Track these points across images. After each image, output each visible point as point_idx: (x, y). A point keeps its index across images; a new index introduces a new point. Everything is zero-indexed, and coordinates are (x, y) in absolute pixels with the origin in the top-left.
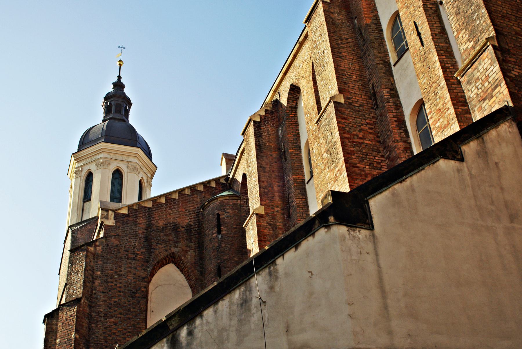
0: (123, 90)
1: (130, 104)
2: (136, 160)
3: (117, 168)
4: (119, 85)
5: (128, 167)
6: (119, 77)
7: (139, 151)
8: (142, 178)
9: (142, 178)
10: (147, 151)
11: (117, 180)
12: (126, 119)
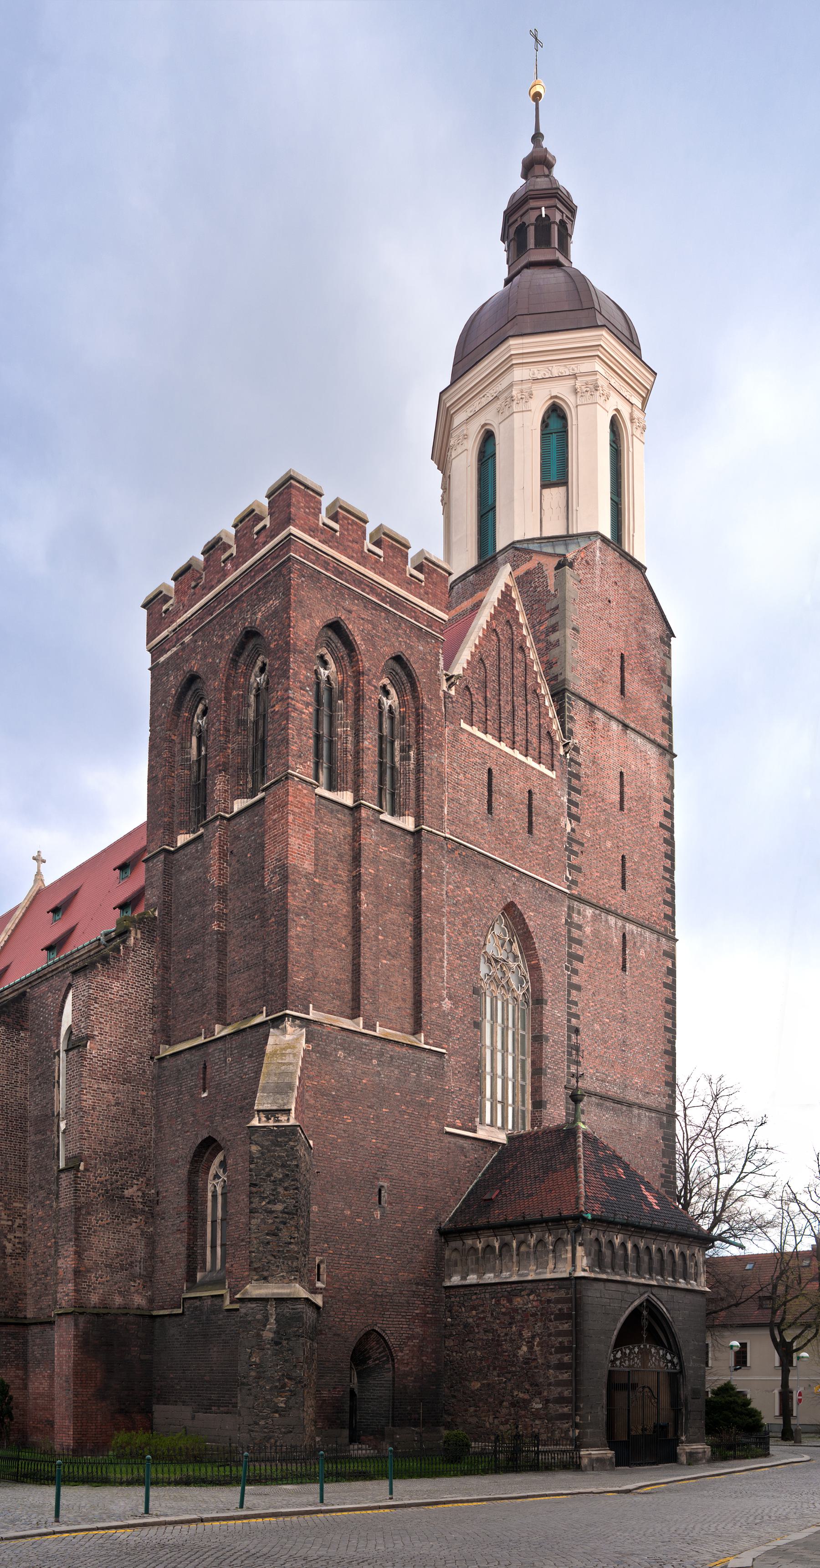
2: (598, 366)
7: (605, 338)
8: (617, 410)
10: (627, 334)
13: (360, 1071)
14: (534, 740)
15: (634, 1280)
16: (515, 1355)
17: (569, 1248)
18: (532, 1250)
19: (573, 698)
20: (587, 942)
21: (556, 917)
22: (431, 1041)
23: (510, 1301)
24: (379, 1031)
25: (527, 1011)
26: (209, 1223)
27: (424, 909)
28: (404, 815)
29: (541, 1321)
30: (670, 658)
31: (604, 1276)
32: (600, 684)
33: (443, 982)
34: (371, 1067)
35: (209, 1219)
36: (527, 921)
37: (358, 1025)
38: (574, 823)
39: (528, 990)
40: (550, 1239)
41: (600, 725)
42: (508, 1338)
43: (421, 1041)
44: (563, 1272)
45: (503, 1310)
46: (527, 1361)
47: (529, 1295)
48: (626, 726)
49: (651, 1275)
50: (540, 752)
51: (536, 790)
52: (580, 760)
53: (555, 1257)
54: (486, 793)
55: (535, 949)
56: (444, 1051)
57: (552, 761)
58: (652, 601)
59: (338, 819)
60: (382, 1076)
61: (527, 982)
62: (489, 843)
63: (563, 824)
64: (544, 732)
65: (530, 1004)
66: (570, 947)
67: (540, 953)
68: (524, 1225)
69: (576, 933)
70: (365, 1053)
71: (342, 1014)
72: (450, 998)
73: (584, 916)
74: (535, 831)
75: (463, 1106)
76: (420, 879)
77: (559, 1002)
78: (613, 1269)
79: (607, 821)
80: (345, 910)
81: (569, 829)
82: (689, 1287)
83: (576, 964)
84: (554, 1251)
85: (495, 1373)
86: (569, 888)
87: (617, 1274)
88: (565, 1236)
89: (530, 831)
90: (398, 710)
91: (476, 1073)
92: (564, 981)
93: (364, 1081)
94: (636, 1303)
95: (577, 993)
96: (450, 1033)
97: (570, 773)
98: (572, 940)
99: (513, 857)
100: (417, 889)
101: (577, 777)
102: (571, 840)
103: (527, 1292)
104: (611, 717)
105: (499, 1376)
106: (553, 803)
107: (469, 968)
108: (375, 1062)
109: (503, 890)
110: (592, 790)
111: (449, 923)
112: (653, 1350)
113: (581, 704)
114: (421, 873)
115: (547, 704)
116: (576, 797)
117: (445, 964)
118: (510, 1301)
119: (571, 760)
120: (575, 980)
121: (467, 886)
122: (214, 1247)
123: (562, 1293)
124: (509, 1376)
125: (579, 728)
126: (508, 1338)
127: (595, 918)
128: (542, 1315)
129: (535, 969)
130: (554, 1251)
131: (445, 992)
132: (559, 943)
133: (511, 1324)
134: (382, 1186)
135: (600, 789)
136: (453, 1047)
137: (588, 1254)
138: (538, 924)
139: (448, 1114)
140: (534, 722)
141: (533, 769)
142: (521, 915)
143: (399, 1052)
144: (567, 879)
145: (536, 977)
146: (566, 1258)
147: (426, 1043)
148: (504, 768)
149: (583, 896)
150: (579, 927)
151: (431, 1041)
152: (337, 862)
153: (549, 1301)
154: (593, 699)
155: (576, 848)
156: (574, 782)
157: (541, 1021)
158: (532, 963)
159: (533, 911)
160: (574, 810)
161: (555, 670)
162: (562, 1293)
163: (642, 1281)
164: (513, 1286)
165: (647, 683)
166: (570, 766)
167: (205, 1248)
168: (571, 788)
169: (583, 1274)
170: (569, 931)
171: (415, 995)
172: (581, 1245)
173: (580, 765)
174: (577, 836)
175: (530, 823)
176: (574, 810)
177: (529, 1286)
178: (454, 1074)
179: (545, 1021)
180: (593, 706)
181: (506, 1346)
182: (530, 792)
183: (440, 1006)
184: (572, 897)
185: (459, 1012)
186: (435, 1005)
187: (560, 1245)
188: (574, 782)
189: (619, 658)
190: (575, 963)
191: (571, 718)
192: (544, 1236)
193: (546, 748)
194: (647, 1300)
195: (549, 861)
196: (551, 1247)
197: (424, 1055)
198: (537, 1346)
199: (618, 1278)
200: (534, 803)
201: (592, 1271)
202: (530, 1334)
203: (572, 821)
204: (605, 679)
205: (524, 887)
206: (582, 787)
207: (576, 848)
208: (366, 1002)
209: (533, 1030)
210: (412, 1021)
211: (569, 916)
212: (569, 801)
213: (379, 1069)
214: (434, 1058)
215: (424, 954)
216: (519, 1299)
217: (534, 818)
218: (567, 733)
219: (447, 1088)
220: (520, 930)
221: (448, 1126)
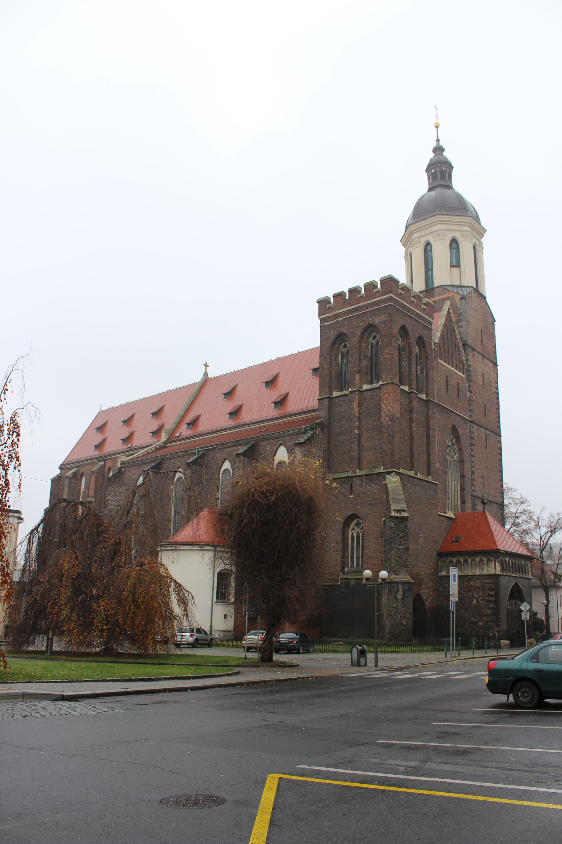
0: (443, 153)
1: (452, 168)
3: (453, 238)
4: (438, 150)
5: (462, 236)
6: (438, 141)
9: (475, 243)
11: (454, 249)
12: (450, 185)
14: (458, 363)
15: (513, 575)
16: (471, 604)
17: (493, 563)
18: (477, 563)
19: (468, 347)
20: (475, 438)
22: (433, 479)
23: (468, 582)
24: (419, 476)
25: (458, 465)
26: (350, 548)
27: (430, 429)
28: (422, 393)
29: (482, 590)
30: (494, 329)
31: (504, 574)
32: (476, 341)
35: (350, 546)
36: (459, 432)
37: (412, 473)
40: (485, 559)
41: (476, 356)
42: (468, 597)
43: (430, 479)
44: (492, 572)
45: (466, 586)
46: (476, 606)
47: (476, 580)
48: (483, 356)
49: (516, 572)
50: (460, 368)
51: (459, 382)
52: (471, 370)
53: (487, 566)
55: (461, 442)
56: (437, 483)
57: (463, 371)
58: (489, 309)
61: (458, 454)
63: (467, 394)
64: (461, 361)
66: (471, 441)
67: (463, 444)
68: (474, 553)
69: (472, 435)
71: (407, 469)
74: (460, 398)
76: (429, 418)
78: (506, 571)
81: (469, 396)
82: (527, 577)
84: (487, 564)
85: (462, 611)
86: (470, 418)
87: (508, 573)
88: (491, 558)
89: (458, 398)
91: (445, 491)
94: (513, 584)
97: (469, 375)
98: (472, 438)
100: (428, 421)
101: (470, 376)
102: (470, 400)
103: (476, 579)
104: (479, 353)
105: (464, 612)
111: (437, 434)
112: (518, 602)
113: (471, 349)
114: (429, 416)
115: (461, 350)
116: (471, 384)
118: (468, 582)
120: (473, 453)
122: (352, 558)
123: (491, 580)
124: (469, 612)
125: (470, 358)
126: (468, 597)
128: (482, 588)
129: (460, 449)
130: (487, 564)
131: (437, 460)
133: (469, 592)
134: (421, 537)
137: (500, 566)
140: (458, 357)
141: (459, 374)
142: (457, 429)
146: (492, 567)
147: (432, 480)
149: (474, 421)
150: (473, 433)
151: (433, 479)
153: (485, 583)
154: (473, 347)
155: (471, 403)
156: (470, 378)
157: (463, 470)
160: (470, 388)
162: (491, 580)
163: (514, 575)
164: (470, 577)
167: (348, 558)
169: (499, 573)
170: (470, 435)
171: (427, 461)
172: (498, 562)
173: (471, 371)
175: (458, 394)
176: (470, 388)
177: (477, 577)
178: (440, 492)
179: (465, 470)
180: (474, 350)
181: (467, 600)
182: (458, 383)
183: (436, 466)
184: (471, 421)
185: (441, 468)
186: (434, 465)
187: (489, 562)
189: (480, 331)
190: (472, 446)
191: (468, 354)
192: (482, 558)
193: (461, 366)
194: (516, 583)
196: (485, 563)
197: (432, 485)
198: (481, 600)
199: (508, 574)
200: (459, 387)
201: (501, 572)
202: (477, 596)
204: (477, 339)
205: (458, 419)
207: (471, 403)
209: (460, 473)
210: (426, 471)
211: (470, 429)
212: (469, 386)
214: (435, 486)
215: (431, 446)
216: (472, 582)
218: (467, 360)
221: (439, 512)
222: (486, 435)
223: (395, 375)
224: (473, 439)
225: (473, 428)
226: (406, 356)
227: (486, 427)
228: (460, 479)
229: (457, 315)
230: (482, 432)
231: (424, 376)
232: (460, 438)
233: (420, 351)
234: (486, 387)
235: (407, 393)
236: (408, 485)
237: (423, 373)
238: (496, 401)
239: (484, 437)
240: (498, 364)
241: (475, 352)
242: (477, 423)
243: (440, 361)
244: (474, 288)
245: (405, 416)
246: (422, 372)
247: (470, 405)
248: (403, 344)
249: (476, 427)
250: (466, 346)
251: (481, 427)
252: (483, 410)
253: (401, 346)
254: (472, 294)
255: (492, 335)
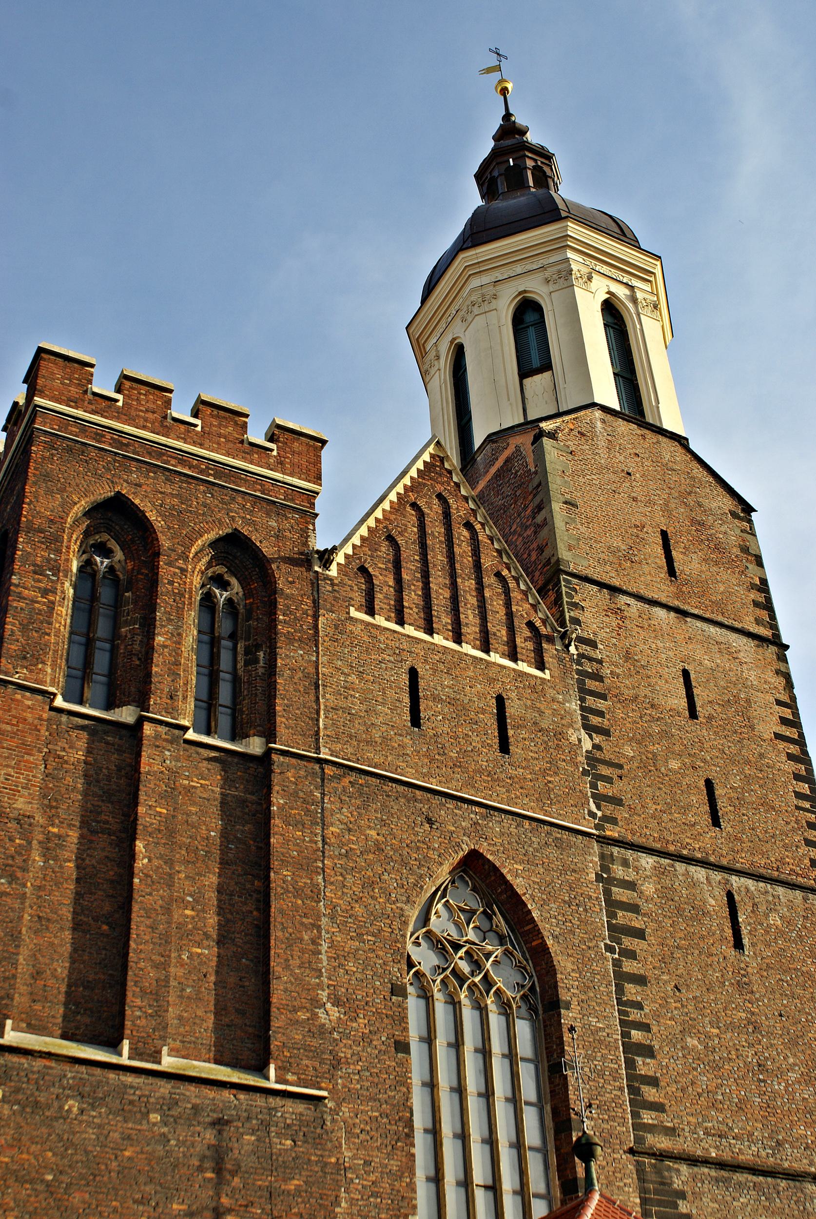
13: (116, 1136)
20: (645, 907)
21: (574, 871)
22: (290, 1077)
24: (168, 1062)
28: (248, 736)
33: (320, 976)
34: (145, 1127)
36: (509, 877)
38: (598, 739)
39: (532, 989)
48: (683, 613)
54: (407, 700)
59: (107, 743)
60: (173, 1142)
61: (531, 977)
62: (415, 766)
63: (573, 739)
65: (541, 1012)
69: (620, 894)
70: (131, 1102)
72: (337, 1003)
73: (637, 869)
75: (375, 1195)
77: (599, 1004)
79: (665, 734)
80: (112, 873)
83: (628, 942)
86: (597, 827)
89: (504, 747)
90: (242, 603)
92: (607, 971)
93: (127, 1154)
95: (639, 988)
96: (336, 1064)
99: (470, 784)
101: (597, 677)
106: (548, 712)
107: (381, 953)
108: (155, 1117)
109: (452, 833)
110: (628, 693)
117: (324, 947)
119: (581, 656)
120: (629, 966)
121: (369, 827)
127: (660, 872)
131: (323, 995)
132: (586, 910)
135: (643, 692)
136: (344, 1086)
138: (534, 882)
139: (338, 1210)
142: (496, 869)
143: (214, 1099)
144: (592, 815)
145: (544, 966)
148: (441, 666)
149: (630, 837)
151: (290, 1077)
152: (100, 803)
154: (616, 582)
155: (605, 771)
156: (591, 684)
158: (534, 944)
159: (521, 862)
160: (595, 720)
161: (547, 553)
165: (716, 564)
166: (579, 663)
168: (584, 692)
174: (607, 755)
176: (595, 720)
180: (614, 590)
184: (604, 840)
188: (591, 684)
195: (549, 790)
197: (274, 1101)
203: (594, 735)
205: (495, 826)
206: (609, 690)
207: (605, 771)
208: (138, 1013)
211: (605, 868)
212: (582, 708)
213: (165, 1130)
214: (301, 1107)
217: (511, 732)
219: (333, 1160)
220: (501, 893)
222: (730, 895)
223: (25, 658)
224: (634, 908)
225: (625, 863)
226: (135, 603)
227: (724, 862)
228: (551, 1082)
229: (530, 497)
230: (694, 884)
231: (261, 671)
232: (526, 905)
233: (248, 593)
234: (710, 718)
235: (124, 732)
236: (72, 1105)
237: (256, 661)
238: (790, 767)
239: (715, 902)
240: (785, 641)
241: (623, 599)
242: (658, 846)
243: (354, 613)
244: (605, 409)
245: (103, 817)
246: (252, 661)
247: (608, 780)
248: (130, 566)
249: (648, 861)
250: (563, 577)
251: (689, 860)
252: (699, 799)
253: (121, 576)
254: (599, 424)
255: (736, 551)
